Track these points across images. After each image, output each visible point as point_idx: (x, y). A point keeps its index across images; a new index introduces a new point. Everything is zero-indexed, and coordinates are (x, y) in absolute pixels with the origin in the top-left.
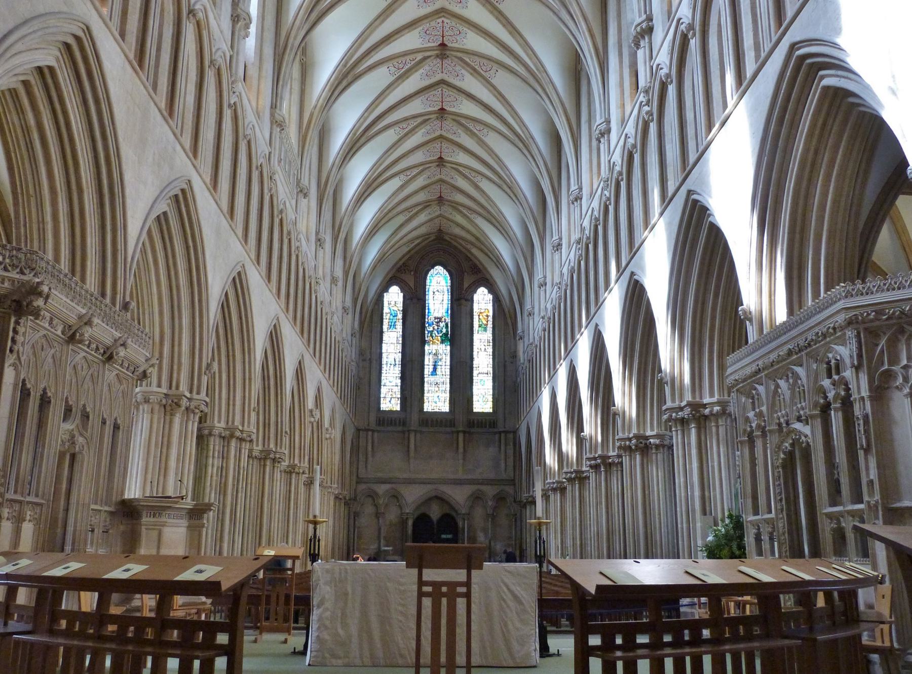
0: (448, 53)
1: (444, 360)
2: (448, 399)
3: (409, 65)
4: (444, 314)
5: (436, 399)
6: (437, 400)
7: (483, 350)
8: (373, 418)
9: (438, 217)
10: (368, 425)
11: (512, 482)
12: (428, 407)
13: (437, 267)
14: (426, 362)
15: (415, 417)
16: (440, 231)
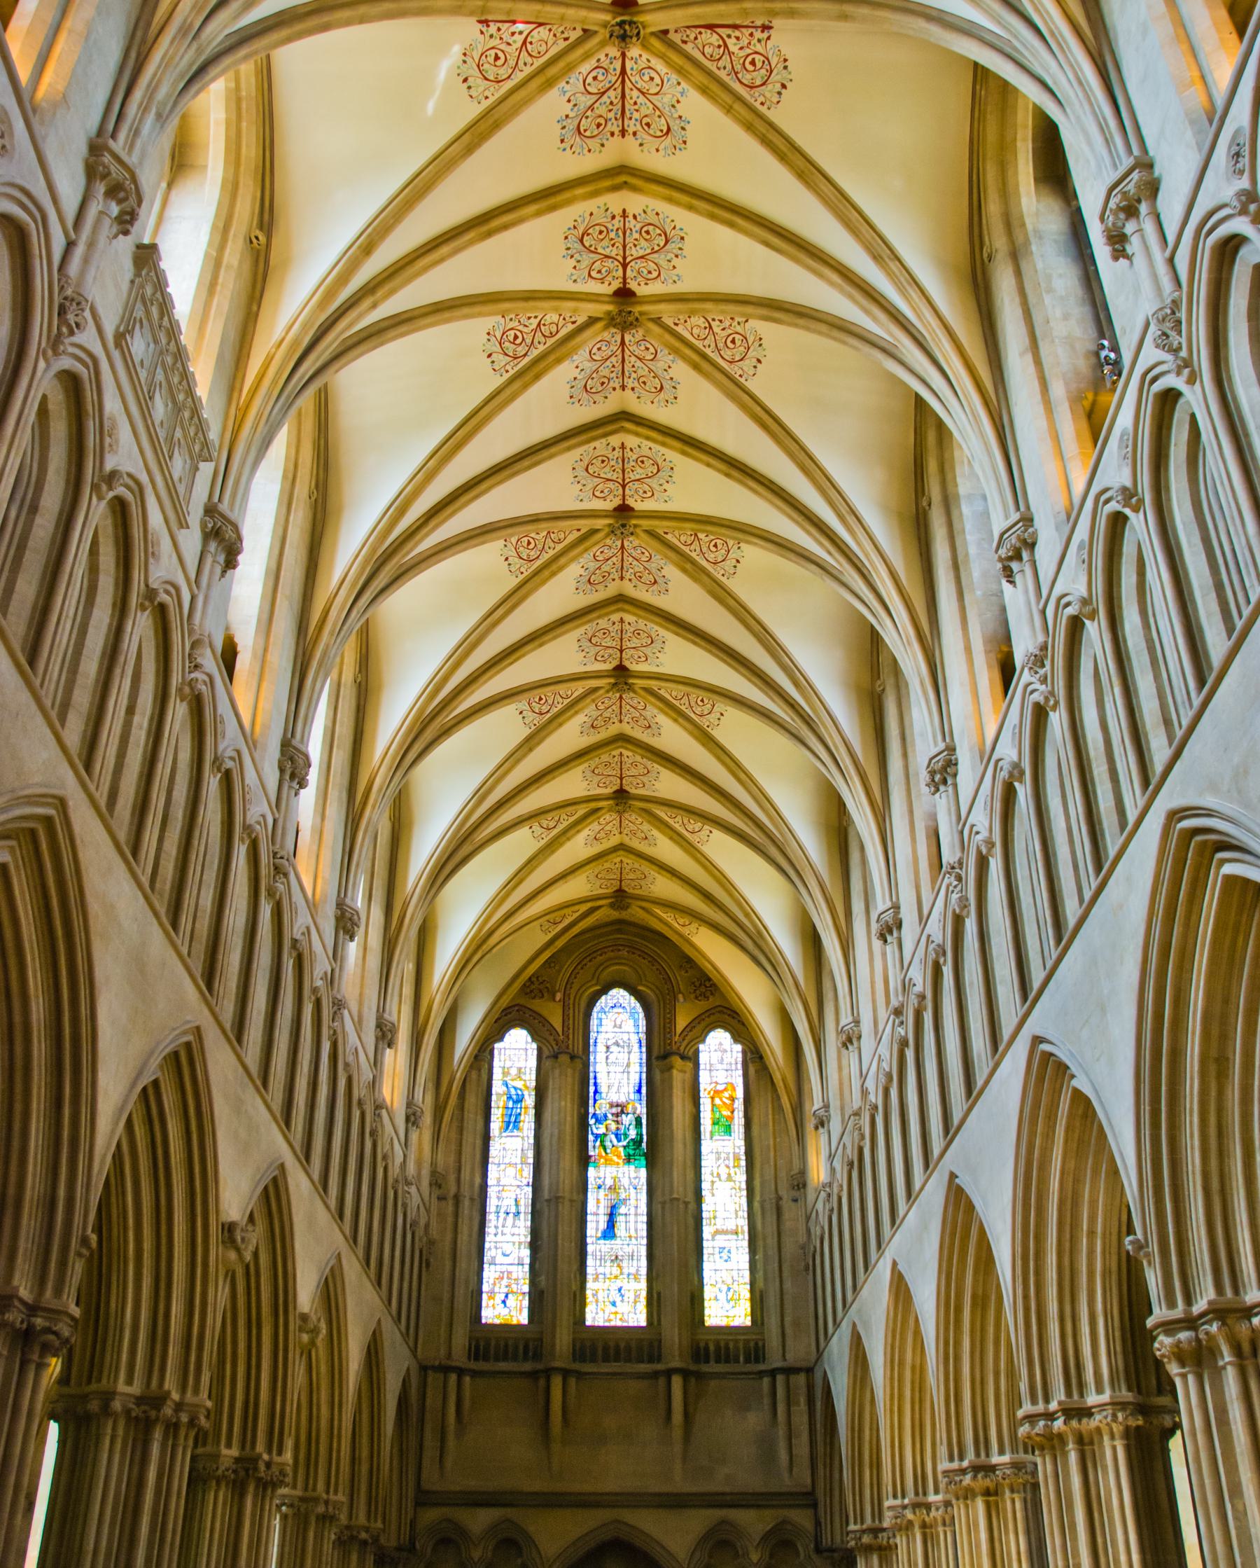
0: (637, 309)
1: (633, 1202)
2: (644, 1294)
3: (541, 348)
4: (632, 1097)
5: (615, 1296)
6: (618, 1299)
7: (724, 1177)
8: (460, 1340)
9: (615, 849)
10: (449, 1355)
11: (808, 1500)
12: (595, 1316)
13: (614, 992)
14: (591, 1207)
15: (563, 1340)
16: (620, 897)
